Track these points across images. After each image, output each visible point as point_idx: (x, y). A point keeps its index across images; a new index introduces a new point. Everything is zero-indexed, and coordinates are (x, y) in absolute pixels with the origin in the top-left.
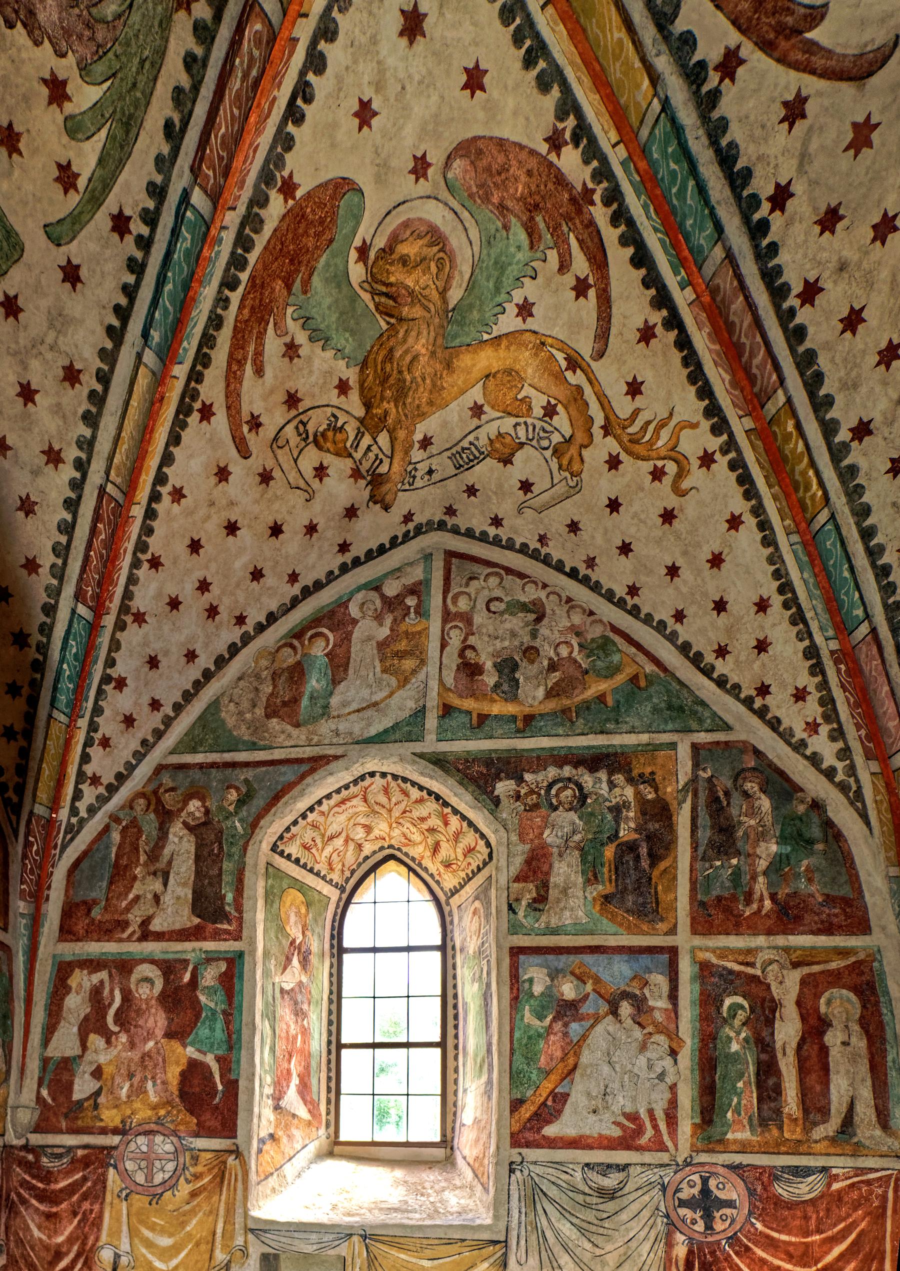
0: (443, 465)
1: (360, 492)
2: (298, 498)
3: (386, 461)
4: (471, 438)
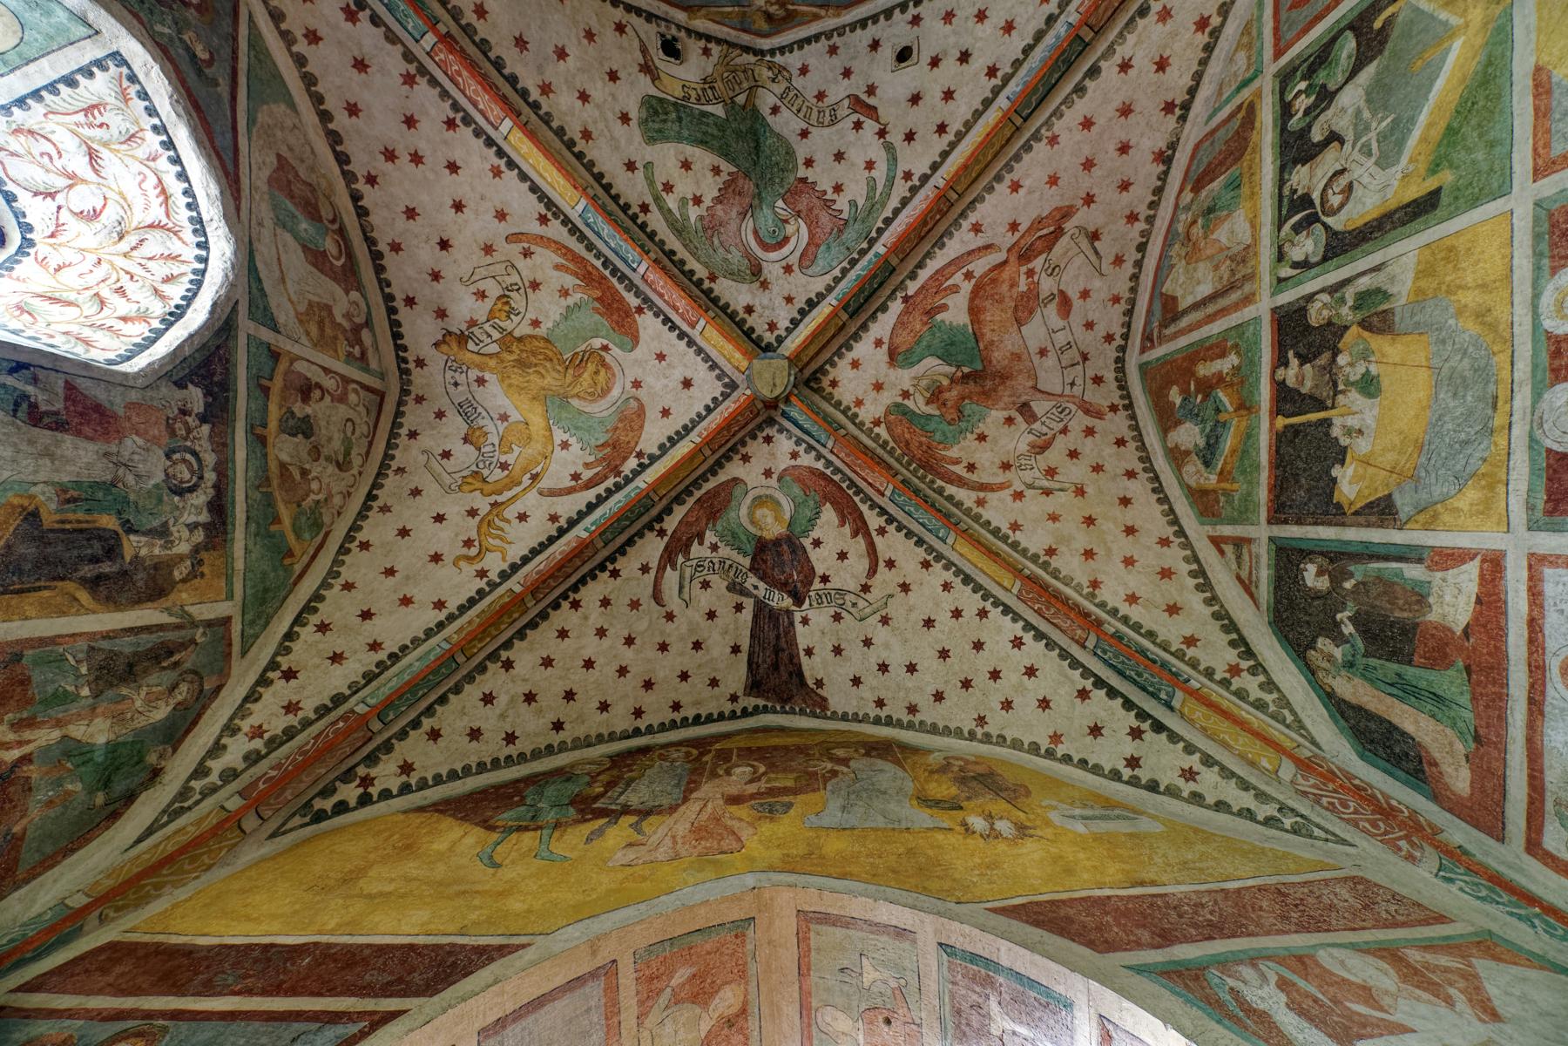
0: (460, 394)
1: (457, 324)
2: (465, 270)
3: (476, 349)
4: (484, 413)
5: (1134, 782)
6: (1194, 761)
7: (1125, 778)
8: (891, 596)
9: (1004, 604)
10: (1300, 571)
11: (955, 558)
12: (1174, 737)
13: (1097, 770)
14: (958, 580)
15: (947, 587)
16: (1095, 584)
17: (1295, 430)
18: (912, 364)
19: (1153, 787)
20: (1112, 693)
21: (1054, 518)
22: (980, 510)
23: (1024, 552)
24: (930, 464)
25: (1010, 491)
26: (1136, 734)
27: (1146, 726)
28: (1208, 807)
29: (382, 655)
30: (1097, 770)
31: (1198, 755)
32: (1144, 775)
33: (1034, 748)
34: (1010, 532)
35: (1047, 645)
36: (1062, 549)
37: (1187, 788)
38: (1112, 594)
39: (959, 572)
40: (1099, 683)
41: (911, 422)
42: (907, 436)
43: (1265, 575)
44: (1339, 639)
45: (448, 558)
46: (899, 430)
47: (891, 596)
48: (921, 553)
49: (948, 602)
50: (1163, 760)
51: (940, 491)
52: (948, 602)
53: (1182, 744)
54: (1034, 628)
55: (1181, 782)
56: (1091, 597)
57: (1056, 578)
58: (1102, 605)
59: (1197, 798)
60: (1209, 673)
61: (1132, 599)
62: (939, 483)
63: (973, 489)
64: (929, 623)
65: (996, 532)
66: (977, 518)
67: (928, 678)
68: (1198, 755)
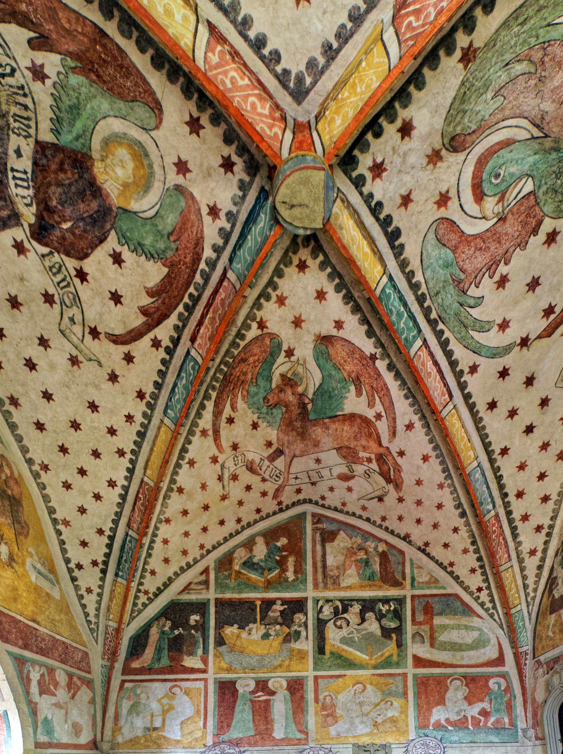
5: (70, 571)
6: (97, 590)
7: (69, 566)
10: (196, 613)
11: (155, 421)
12: (103, 579)
13: (64, 551)
14: (139, 428)
17: (254, 610)
18: (317, 359)
19: (74, 579)
24: (229, 384)
28: (80, 602)
30: (64, 551)
32: (76, 573)
33: (51, 511)
37: (83, 592)
39: (145, 427)
41: (265, 361)
42: (251, 360)
43: (193, 597)
44: (172, 629)
46: (256, 350)
48: (149, 389)
49: (119, 423)
51: (207, 397)
52: (119, 423)
59: (81, 597)
60: (141, 584)
62: (214, 395)
64: (93, 407)
67: (50, 414)
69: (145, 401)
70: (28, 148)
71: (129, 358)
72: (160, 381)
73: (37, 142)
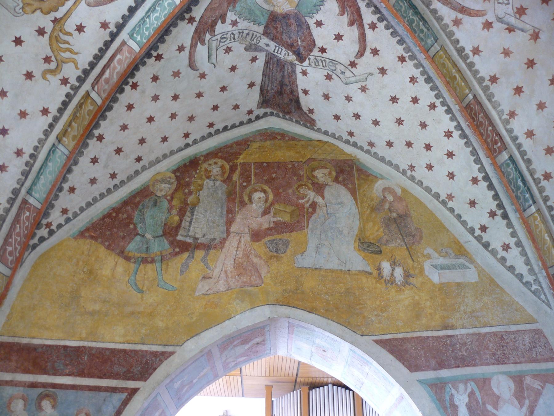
5: (479, 239)
7: (476, 235)
8: (371, 74)
9: (448, 106)
15: (413, 80)
16: (512, 114)
19: (486, 246)
20: (491, 187)
21: (507, 53)
22: (454, 29)
23: (475, 73)
25: (482, 20)
26: (492, 214)
27: (499, 212)
29: (26, 157)
31: (515, 239)
34: (471, 54)
35: (466, 143)
36: (502, 80)
37: (502, 253)
38: (519, 127)
40: (486, 178)
45: (37, 74)
47: (371, 74)
50: (499, 233)
53: (511, 230)
54: (462, 130)
55: (500, 249)
56: (506, 122)
57: (490, 100)
58: (510, 131)
59: (503, 260)
61: (530, 134)
63: (454, 9)
65: (460, 51)
66: (450, 35)
68: (515, 239)
69: (407, 59)
70: (265, 40)
71: (375, 52)
72: (398, 38)
73: (263, 35)
